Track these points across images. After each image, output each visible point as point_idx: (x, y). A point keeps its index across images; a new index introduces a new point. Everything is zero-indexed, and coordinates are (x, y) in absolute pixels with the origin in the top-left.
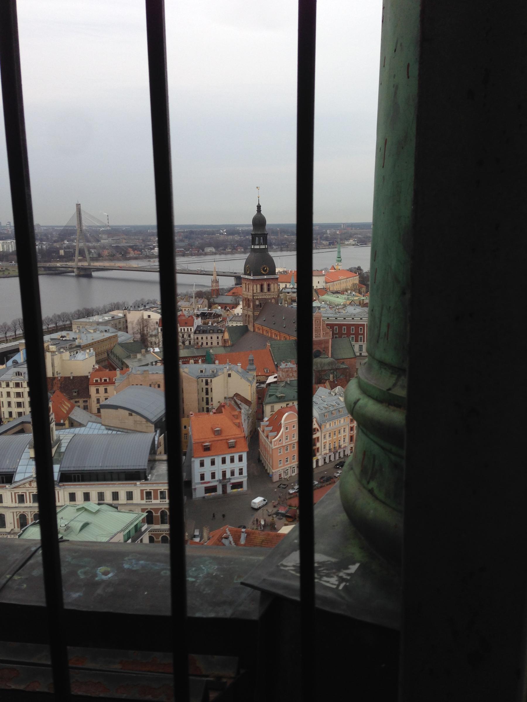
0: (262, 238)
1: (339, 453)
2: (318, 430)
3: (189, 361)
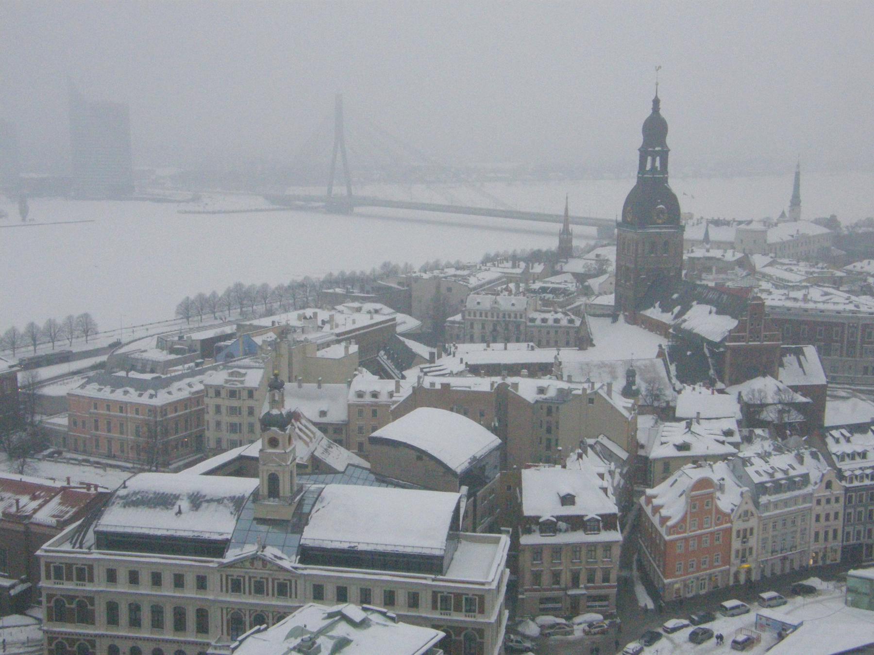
0: (658, 159)
1: (792, 560)
2: (752, 515)
3: (520, 371)
